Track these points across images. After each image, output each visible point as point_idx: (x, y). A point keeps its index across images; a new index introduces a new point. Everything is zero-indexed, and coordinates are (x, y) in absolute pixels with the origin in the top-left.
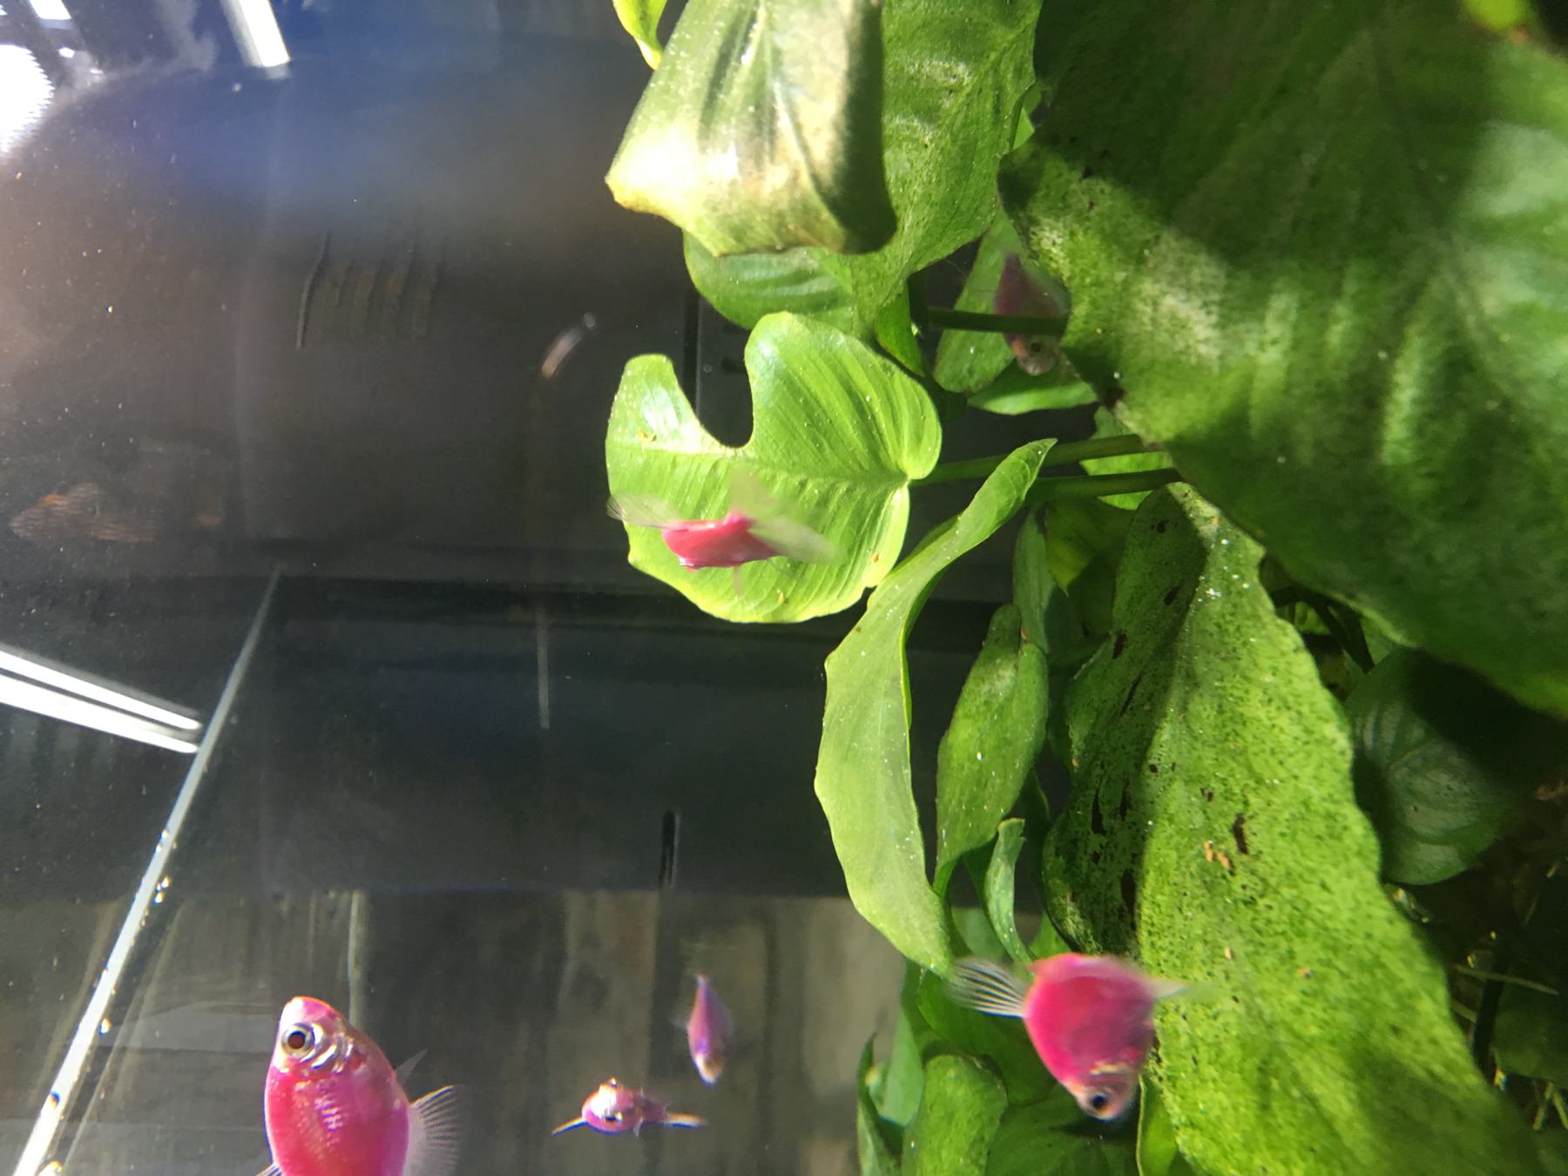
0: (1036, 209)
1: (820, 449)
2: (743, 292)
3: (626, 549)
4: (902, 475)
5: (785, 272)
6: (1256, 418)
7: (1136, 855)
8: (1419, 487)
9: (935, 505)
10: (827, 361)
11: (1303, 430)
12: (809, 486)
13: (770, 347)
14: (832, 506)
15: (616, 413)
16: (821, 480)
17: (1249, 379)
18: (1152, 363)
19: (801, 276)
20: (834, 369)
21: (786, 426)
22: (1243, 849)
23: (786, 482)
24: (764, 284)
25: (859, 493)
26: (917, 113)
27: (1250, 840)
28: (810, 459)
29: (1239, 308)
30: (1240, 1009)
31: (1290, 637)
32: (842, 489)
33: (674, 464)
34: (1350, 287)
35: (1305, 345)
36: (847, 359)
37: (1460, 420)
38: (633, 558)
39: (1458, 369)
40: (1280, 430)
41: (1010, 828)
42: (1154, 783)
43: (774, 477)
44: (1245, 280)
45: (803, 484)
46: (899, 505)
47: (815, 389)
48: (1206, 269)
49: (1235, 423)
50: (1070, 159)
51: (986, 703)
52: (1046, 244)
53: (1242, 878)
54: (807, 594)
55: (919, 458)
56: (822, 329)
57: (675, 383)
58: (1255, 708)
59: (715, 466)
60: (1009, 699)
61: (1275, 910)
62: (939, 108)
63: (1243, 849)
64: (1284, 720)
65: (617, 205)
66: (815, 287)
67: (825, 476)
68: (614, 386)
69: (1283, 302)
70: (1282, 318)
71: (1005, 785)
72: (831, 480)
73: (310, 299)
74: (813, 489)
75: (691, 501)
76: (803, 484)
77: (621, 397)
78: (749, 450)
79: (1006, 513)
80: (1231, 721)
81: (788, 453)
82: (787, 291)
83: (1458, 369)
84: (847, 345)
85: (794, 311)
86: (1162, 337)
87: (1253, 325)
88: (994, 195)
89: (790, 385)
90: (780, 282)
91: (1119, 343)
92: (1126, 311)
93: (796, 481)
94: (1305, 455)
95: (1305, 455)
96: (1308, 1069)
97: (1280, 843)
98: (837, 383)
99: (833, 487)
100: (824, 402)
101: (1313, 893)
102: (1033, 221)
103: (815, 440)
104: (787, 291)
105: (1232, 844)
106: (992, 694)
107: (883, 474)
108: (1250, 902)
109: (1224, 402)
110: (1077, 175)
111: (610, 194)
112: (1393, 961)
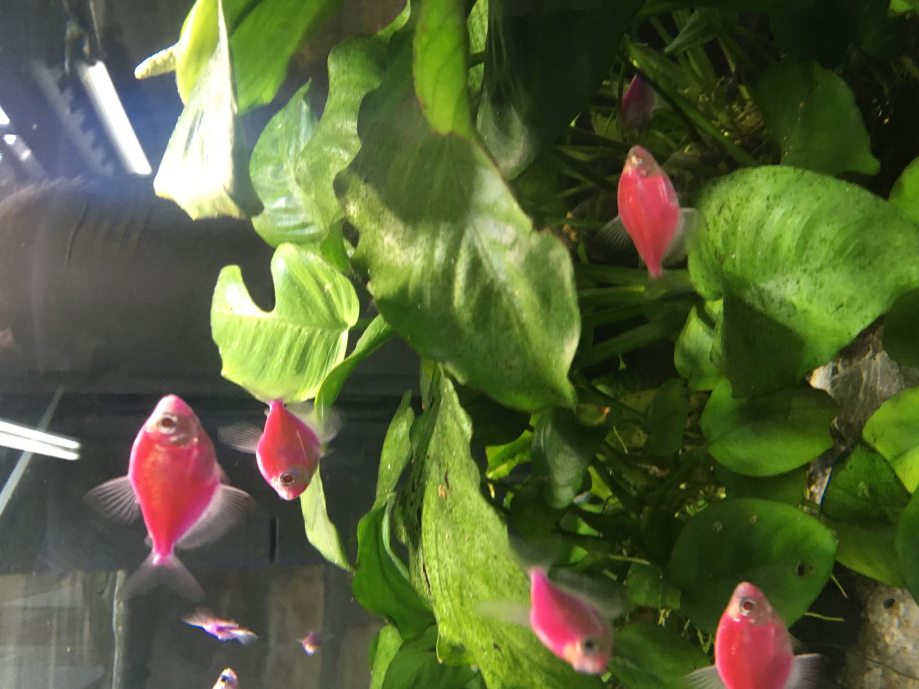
0: (349, 197)
1: (307, 313)
2: (278, 233)
3: (221, 367)
4: (344, 325)
5: (297, 223)
6: (411, 289)
7: (422, 500)
8: (466, 316)
9: (355, 335)
10: (307, 267)
11: (428, 294)
12: (303, 331)
13: (283, 263)
14: (314, 342)
15: (216, 297)
16: (308, 328)
17: (411, 272)
18: (382, 265)
19: (304, 226)
20: (310, 271)
21: (290, 300)
22: (448, 486)
23: (292, 330)
24: (288, 229)
25: (326, 335)
26: (341, 146)
27: (450, 482)
28: (303, 318)
29: (410, 241)
30: (452, 561)
31: (450, 386)
32: (318, 332)
33: (240, 322)
34: (442, 233)
35: (429, 258)
36: (315, 266)
37: (478, 289)
38: (226, 372)
39: (476, 266)
40: (419, 294)
41: (390, 498)
42: (428, 463)
43: (286, 328)
44: (409, 229)
45: (300, 330)
46: (344, 337)
47: (303, 281)
48: (400, 226)
49: (404, 290)
50: (360, 175)
51: (395, 440)
52: (352, 213)
53: (449, 500)
54: (305, 387)
55: (351, 317)
56: (303, 252)
57: (241, 279)
58: (449, 422)
59: (259, 322)
60: (403, 438)
61: (457, 512)
62: (350, 145)
63: (448, 486)
64: (455, 425)
65: (157, 197)
66: (311, 231)
67: (311, 325)
68: (214, 283)
69: (422, 239)
70: (421, 245)
71: (395, 476)
72: (313, 328)
73: (74, 238)
74: (305, 333)
75: (249, 340)
76: (300, 330)
77: (218, 288)
78: (274, 314)
79: (373, 338)
80: (444, 427)
81: (292, 314)
82: (298, 232)
83: (476, 266)
84: (314, 258)
85: (291, 242)
86: (385, 254)
87: (413, 249)
88: (332, 193)
89: (292, 281)
90: (295, 228)
91: (371, 257)
92: (375, 243)
93: (296, 329)
94: (428, 303)
95: (428, 303)
96: (473, 583)
97: (457, 481)
98: (312, 279)
99: (314, 332)
100: (307, 288)
101: (467, 502)
102: (347, 202)
103: (304, 307)
104: (298, 232)
105: (445, 487)
106: (397, 436)
107: (338, 324)
108: (451, 510)
109: (401, 282)
110: (362, 182)
111: (153, 191)
112: (490, 525)
